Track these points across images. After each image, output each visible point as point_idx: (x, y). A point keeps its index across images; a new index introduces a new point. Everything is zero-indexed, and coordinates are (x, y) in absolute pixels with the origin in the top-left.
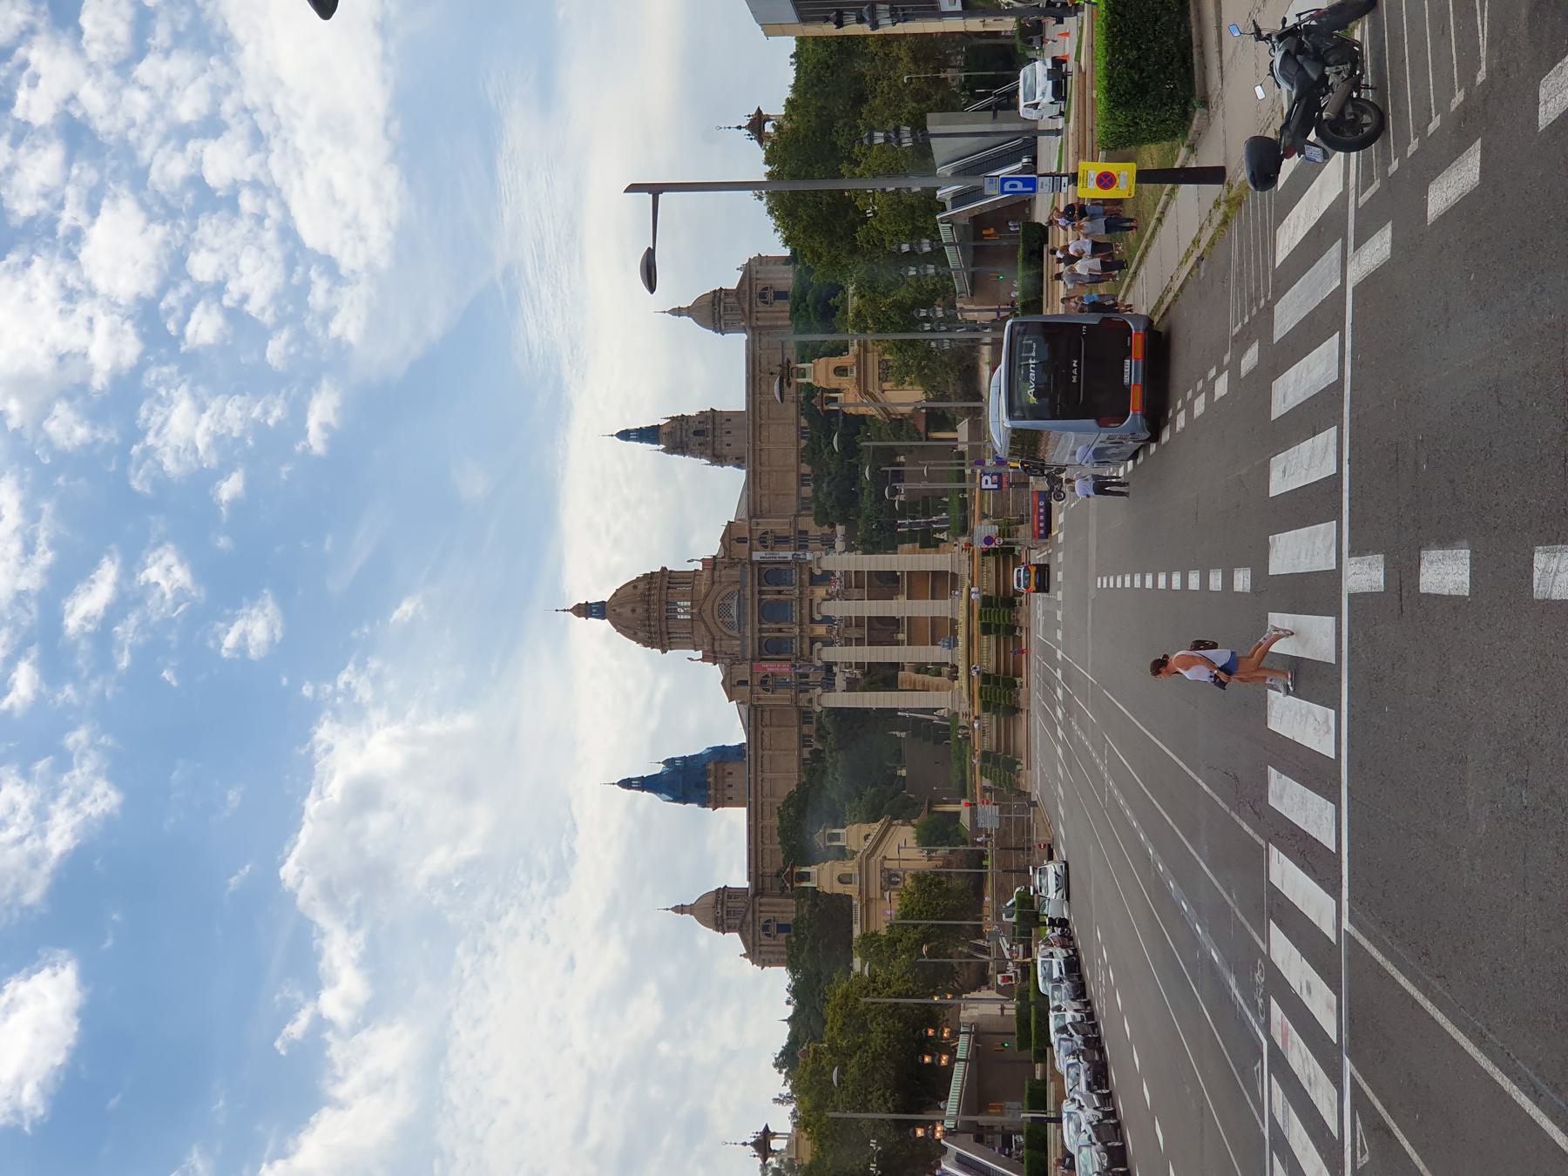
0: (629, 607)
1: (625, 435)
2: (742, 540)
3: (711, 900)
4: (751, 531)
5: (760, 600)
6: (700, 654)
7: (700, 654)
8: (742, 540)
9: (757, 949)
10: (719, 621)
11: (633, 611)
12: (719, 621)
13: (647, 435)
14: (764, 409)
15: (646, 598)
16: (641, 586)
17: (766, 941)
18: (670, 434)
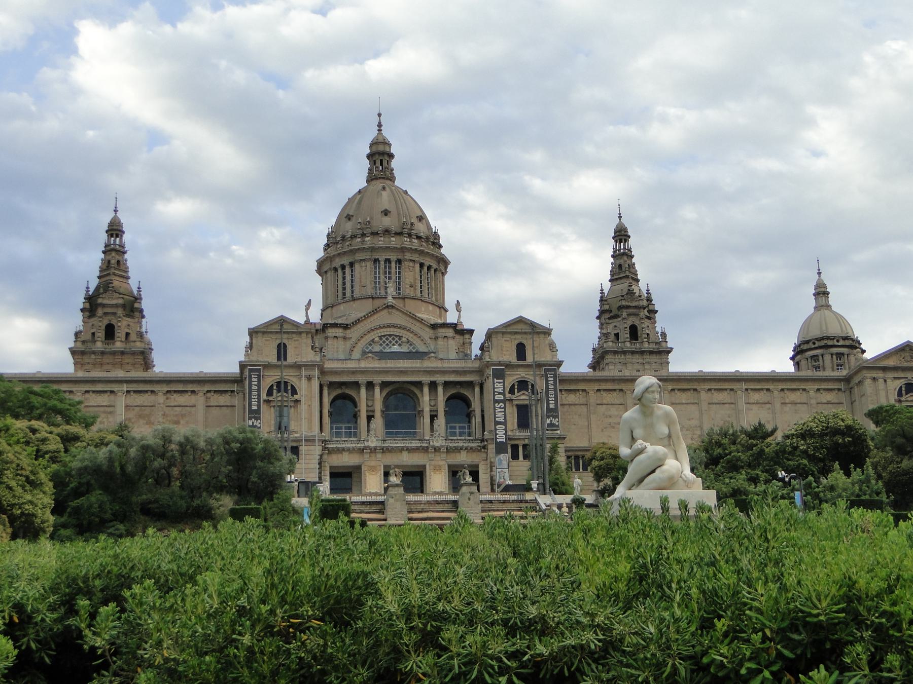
2: (521, 350)
4: (539, 366)
5: (419, 385)
8: (521, 350)
10: (375, 335)
11: (386, 213)
13: (623, 266)
18: (630, 293)
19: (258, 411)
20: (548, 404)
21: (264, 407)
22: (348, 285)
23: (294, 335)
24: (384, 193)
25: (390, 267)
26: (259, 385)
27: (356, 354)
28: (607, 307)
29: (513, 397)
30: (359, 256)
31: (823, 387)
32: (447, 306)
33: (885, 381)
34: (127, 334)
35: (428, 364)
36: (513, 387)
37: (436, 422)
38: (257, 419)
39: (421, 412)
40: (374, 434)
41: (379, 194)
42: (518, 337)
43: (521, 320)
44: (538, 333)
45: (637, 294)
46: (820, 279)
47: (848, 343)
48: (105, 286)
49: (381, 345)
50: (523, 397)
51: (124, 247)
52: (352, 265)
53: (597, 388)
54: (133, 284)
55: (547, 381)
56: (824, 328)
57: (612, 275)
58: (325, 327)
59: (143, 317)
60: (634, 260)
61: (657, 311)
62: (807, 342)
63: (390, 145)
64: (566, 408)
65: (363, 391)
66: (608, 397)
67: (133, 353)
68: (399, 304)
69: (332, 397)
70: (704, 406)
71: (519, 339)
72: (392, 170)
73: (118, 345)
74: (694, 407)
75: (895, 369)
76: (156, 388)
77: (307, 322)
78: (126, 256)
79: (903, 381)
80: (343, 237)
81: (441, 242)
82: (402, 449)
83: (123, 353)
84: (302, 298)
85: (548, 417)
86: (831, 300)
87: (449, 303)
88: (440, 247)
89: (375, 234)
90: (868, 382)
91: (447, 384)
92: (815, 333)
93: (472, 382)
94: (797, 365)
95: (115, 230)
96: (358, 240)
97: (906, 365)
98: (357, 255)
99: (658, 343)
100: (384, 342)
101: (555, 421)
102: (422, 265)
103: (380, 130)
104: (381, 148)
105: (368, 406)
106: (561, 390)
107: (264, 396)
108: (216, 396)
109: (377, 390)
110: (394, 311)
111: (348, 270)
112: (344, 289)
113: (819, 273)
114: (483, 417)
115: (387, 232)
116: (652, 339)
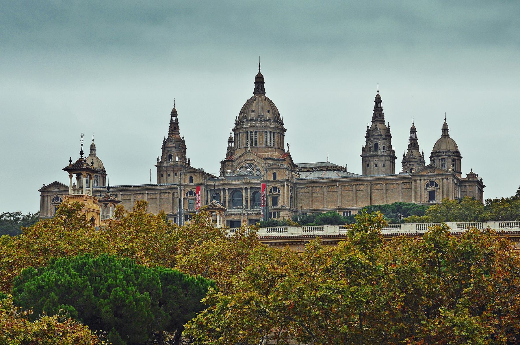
5: (241, 188)
14: (363, 187)
24: (255, 102)
33: (421, 181)
36: (271, 190)
47: (448, 154)
50: (275, 194)
52: (240, 133)
54: (181, 136)
66: (317, 189)
71: (274, 171)
74: (351, 192)
75: (425, 176)
83: (174, 166)
90: (413, 182)
91: (251, 188)
92: (436, 149)
95: (174, 113)
97: (430, 173)
103: (259, 71)
104: (258, 80)
109: (227, 192)
113: (445, 120)
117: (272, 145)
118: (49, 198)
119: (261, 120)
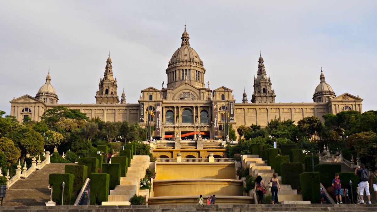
0: (188, 54)
1: (261, 61)
2: (223, 97)
3: (51, 91)
4: (227, 101)
5: (192, 107)
6: (165, 87)
7: (165, 87)
8: (223, 97)
9: (16, 105)
12: (182, 92)
13: (261, 71)
15: (191, 60)
16: (197, 60)
17: (21, 109)
18: (263, 78)
19: (143, 115)
20: (231, 113)
21: (145, 115)
22: (174, 77)
23: (154, 93)
24: (186, 49)
25: (187, 72)
26: (143, 108)
27: (176, 98)
28: (256, 83)
29: (220, 111)
30: (177, 68)
31: (319, 107)
32: (205, 83)
34: (112, 92)
35: (195, 101)
36: (220, 108)
37: (197, 119)
38: (143, 117)
39: (193, 116)
40: (179, 122)
41: (184, 50)
42: (222, 92)
43: (223, 88)
44: (228, 91)
45: (265, 79)
46: (322, 74)
48: (106, 78)
49: (183, 95)
51: (111, 67)
52: (175, 71)
53: (247, 108)
55: (230, 106)
56: (322, 89)
57: (258, 73)
58: (166, 90)
59: (117, 87)
60: (265, 68)
61: (271, 84)
62: (317, 93)
63: (188, 35)
64: (238, 114)
65: (175, 109)
67: (113, 98)
68: (189, 83)
69: (166, 111)
70: (281, 114)
71: (223, 93)
72: (189, 42)
73: (109, 95)
75: (342, 101)
76: (115, 108)
77: (163, 88)
78: (112, 69)
79: (344, 105)
80: (173, 63)
81: (203, 64)
82: (186, 127)
84: (160, 80)
85: (231, 117)
86: (326, 80)
87: (205, 83)
88: (203, 65)
89: (183, 62)
90: (333, 106)
91: (201, 107)
92: (320, 90)
93: (208, 106)
94: (314, 101)
95: (109, 62)
96: (178, 63)
97: (345, 100)
98: (177, 68)
99: (272, 94)
100: (184, 94)
101: (233, 118)
102: (197, 71)
104: (185, 36)
105: (177, 114)
106: (236, 109)
107: (145, 111)
108: (133, 111)
109: (180, 109)
110: (187, 85)
111: (174, 73)
112: (173, 78)
114: (211, 117)
115: (186, 61)
116: (270, 92)
117: (200, 81)
118: (19, 107)
119: (193, 62)
